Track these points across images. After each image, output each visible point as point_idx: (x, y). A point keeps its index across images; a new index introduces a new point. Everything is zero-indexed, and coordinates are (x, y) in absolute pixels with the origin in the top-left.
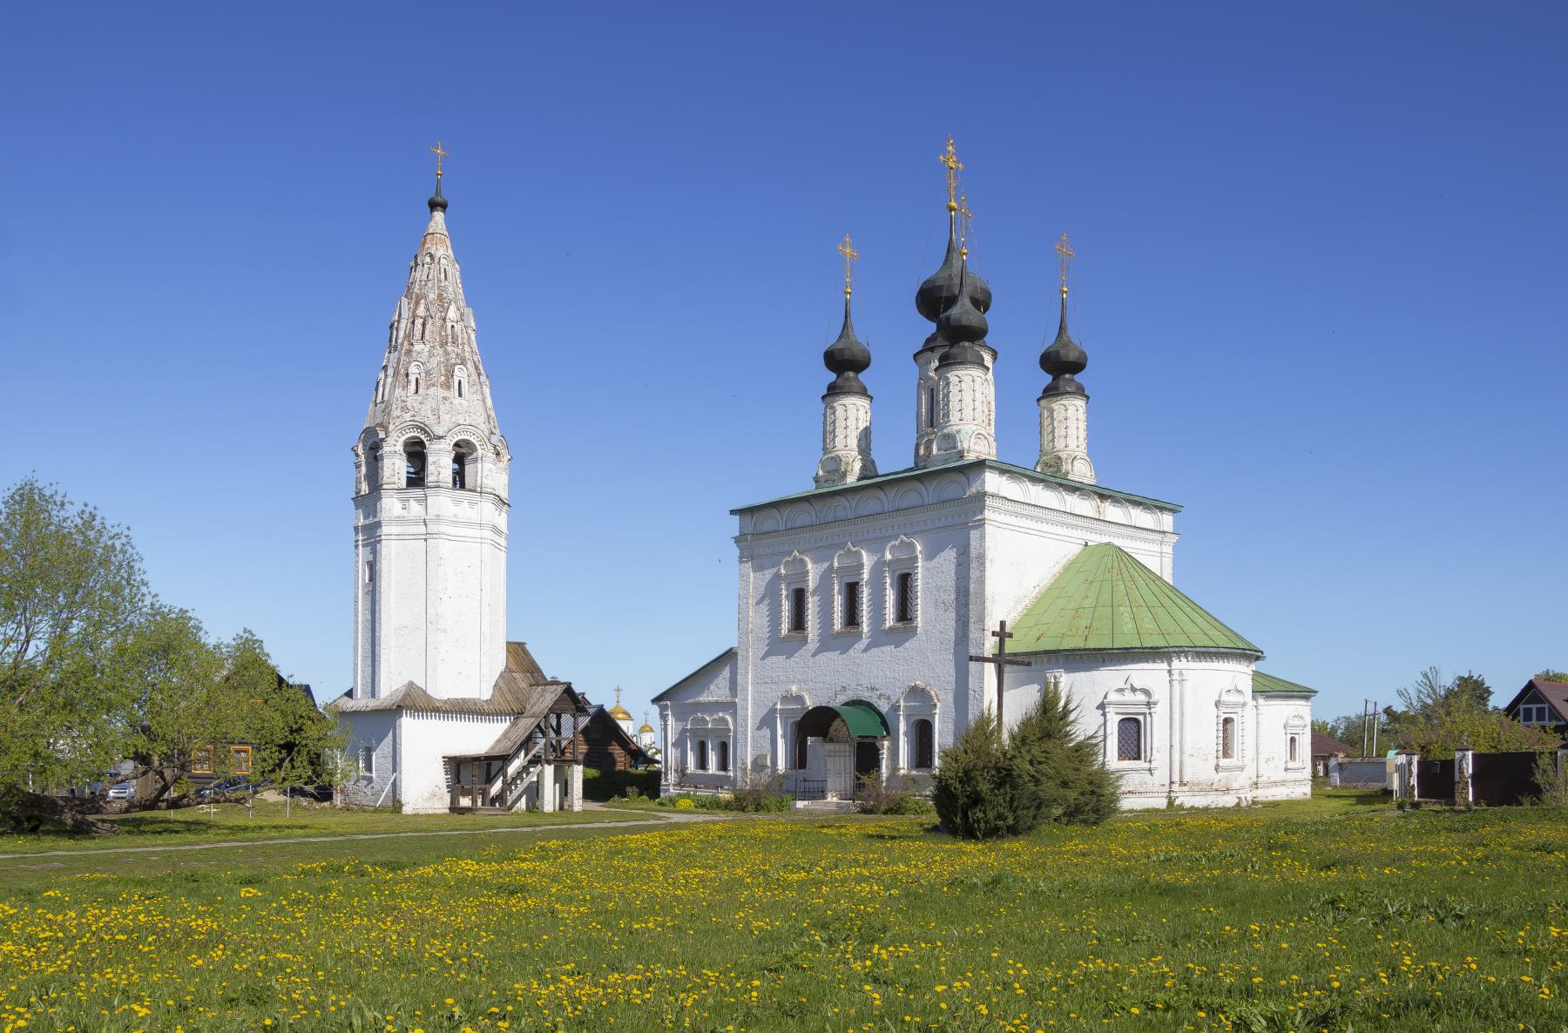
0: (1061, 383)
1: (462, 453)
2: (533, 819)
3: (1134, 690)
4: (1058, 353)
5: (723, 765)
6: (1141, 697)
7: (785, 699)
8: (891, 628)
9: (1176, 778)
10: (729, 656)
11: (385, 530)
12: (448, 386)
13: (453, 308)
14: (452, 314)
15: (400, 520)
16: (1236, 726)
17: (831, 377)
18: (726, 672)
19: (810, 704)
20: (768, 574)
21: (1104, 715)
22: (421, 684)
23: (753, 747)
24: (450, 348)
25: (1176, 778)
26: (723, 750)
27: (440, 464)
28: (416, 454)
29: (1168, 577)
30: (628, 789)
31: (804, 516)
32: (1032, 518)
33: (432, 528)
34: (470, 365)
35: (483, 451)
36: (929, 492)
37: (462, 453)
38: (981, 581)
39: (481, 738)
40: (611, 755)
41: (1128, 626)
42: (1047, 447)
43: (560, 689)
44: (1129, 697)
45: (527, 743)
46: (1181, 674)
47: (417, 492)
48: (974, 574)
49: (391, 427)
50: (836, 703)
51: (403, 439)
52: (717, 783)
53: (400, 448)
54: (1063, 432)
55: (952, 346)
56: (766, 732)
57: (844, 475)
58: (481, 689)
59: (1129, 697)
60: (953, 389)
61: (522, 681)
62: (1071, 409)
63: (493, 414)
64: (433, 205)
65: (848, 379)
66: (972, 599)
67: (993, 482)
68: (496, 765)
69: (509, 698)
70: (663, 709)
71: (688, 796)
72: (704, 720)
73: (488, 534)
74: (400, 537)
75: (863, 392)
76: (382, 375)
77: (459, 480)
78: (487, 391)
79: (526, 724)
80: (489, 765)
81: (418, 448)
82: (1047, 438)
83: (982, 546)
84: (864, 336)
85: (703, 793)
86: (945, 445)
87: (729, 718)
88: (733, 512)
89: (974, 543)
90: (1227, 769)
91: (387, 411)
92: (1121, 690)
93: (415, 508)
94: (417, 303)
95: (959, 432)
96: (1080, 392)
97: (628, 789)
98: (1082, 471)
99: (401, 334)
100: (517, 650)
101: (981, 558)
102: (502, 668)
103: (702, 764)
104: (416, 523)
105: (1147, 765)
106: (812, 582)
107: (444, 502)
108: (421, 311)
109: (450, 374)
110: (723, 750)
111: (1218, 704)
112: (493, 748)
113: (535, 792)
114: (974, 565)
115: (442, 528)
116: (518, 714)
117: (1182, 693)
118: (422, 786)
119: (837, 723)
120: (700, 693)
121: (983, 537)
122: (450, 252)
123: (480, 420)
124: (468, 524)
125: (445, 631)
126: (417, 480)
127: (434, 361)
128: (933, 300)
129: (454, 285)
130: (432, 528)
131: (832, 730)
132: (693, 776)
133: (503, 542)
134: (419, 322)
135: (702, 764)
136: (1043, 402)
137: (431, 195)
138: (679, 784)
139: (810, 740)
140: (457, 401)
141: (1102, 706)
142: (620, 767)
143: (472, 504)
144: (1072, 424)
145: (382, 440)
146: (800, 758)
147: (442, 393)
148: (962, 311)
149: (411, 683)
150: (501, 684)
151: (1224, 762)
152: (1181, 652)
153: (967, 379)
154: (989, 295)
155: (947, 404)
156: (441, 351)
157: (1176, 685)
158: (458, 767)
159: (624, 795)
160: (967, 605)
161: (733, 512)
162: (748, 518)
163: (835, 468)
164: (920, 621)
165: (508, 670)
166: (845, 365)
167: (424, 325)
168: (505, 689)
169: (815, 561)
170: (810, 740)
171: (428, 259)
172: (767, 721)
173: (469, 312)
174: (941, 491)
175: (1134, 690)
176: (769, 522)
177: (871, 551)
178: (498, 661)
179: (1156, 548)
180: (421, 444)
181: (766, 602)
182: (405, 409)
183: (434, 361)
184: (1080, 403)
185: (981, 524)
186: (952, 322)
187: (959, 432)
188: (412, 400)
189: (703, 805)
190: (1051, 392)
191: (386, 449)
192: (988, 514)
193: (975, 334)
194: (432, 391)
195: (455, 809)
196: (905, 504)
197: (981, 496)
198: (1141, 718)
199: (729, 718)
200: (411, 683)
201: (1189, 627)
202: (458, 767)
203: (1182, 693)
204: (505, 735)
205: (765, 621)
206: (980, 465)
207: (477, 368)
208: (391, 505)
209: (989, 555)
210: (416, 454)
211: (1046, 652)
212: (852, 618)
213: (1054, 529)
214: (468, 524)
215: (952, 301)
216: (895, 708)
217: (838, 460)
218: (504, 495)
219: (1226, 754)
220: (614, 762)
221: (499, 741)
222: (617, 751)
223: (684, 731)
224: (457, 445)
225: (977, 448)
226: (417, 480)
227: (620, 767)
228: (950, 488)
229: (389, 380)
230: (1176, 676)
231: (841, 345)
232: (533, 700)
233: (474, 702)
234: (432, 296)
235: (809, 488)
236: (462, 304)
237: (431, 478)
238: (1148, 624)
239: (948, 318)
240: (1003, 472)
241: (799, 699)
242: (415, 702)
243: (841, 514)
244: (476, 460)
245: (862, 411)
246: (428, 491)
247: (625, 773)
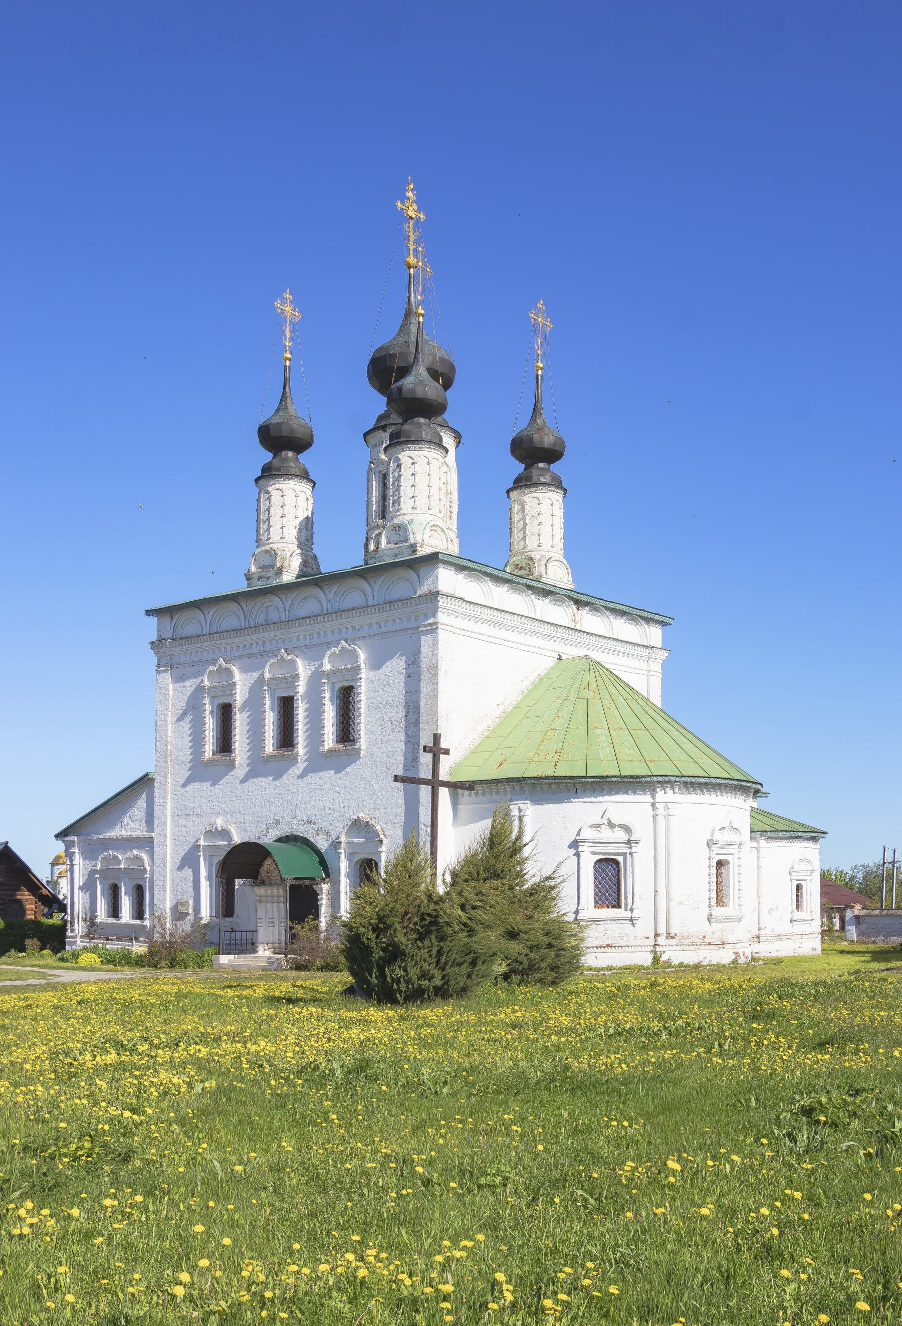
0: (534, 472)
3: (611, 825)
4: (530, 438)
5: (139, 913)
6: (621, 835)
7: (209, 834)
8: (330, 751)
9: (662, 930)
10: (144, 783)
16: (732, 871)
17: (267, 456)
18: (142, 802)
19: (237, 839)
20: (190, 685)
21: (577, 854)
23: (174, 891)
25: (662, 930)
26: (139, 893)
29: (656, 698)
30: (28, 942)
31: (231, 617)
32: (496, 624)
36: (375, 591)
38: (434, 696)
40: (19, 902)
41: (605, 752)
42: (517, 546)
44: (606, 834)
46: (666, 808)
48: (425, 688)
50: (268, 839)
52: (131, 934)
54: (536, 530)
55: (405, 422)
56: (188, 872)
57: (280, 571)
59: (606, 834)
60: (406, 472)
62: (546, 504)
65: (286, 460)
66: (423, 718)
67: (446, 579)
70: (69, 846)
71: (94, 949)
72: (115, 857)
75: (305, 476)
82: (517, 536)
83: (435, 655)
84: (302, 413)
85: (114, 946)
86: (396, 538)
87: (145, 857)
88: (149, 613)
89: (425, 651)
90: (721, 920)
92: (597, 826)
95: (411, 522)
96: (556, 483)
97: (28, 942)
98: (558, 574)
101: (434, 668)
105: (628, 914)
106: (240, 696)
110: (139, 893)
111: (709, 844)
114: (425, 676)
117: (667, 831)
119: (268, 862)
120: (112, 825)
121: (435, 644)
128: (385, 371)
131: (263, 871)
132: (102, 926)
135: (115, 912)
136: (513, 495)
138: (88, 936)
139: (238, 882)
141: (574, 845)
142: (30, 916)
144: (546, 519)
146: (227, 905)
148: (418, 382)
151: (717, 911)
152: (666, 782)
153: (421, 462)
154: (452, 368)
155: (398, 490)
157: (661, 820)
159: (23, 949)
160: (417, 723)
161: (149, 613)
162: (166, 619)
163: (270, 563)
164: (363, 742)
166: (283, 444)
169: (244, 670)
170: (238, 882)
172: (189, 860)
174: (385, 588)
175: (611, 825)
176: (191, 624)
177: (309, 658)
179: (643, 665)
181: (188, 718)
184: (556, 496)
185: (433, 629)
186: (405, 394)
187: (411, 522)
189: (111, 961)
190: (523, 482)
192: (441, 617)
193: (432, 410)
196: (347, 604)
197: (434, 596)
198: (620, 859)
199: (145, 857)
201: (676, 753)
203: (667, 831)
205: (186, 742)
206: (433, 559)
209: (443, 665)
211: (509, 780)
212: (286, 739)
213: (521, 638)
215: (404, 371)
216: (335, 845)
217: (272, 554)
219: (720, 902)
220: (23, 911)
222: (26, 896)
223: (93, 872)
225: (433, 542)
227: (30, 916)
228: (397, 586)
230: (661, 810)
231: (277, 419)
235: (242, 586)
238: (627, 751)
239: (400, 389)
240: (461, 568)
241: (225, 834)
243: (274, 616)
245: (302, 497)
247: (36, 923)
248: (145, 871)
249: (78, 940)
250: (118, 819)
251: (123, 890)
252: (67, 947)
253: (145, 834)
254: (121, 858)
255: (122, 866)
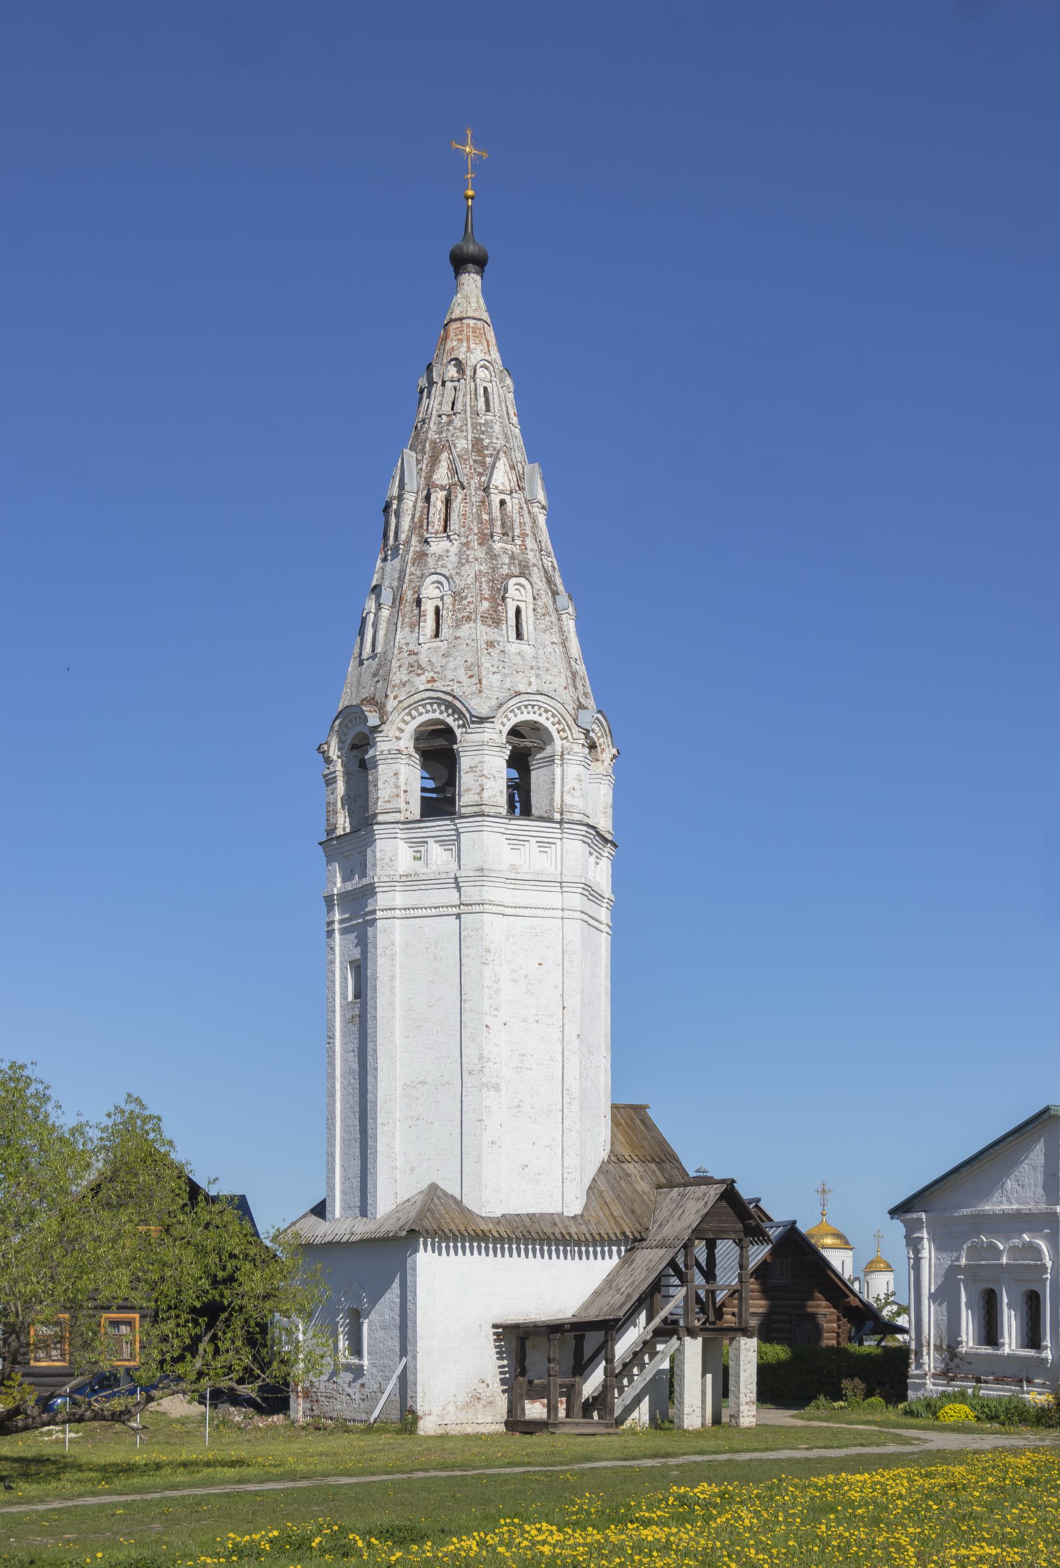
1: (525, 751)
2: (662, 1441)
5: (1032, 1338)
11: (382, 900)
12: (495, 620)
13: (502, 465)
14: (501, 477)
15: (411, 881)
22: (453, 1189)
24: (497, 546)
26: (1032, 1305)
27: (484, 770)
28: (438, 752)
30: (846, 1383)
33: (470, 893)
34: (537, 576)
35: (566, 743)
37: (525, 751)
39: (562, 1288)
40: (813, 1317)
43: (713, 1193)
45: (650, 1297)
47: (441, 826)
49: (391, 704)
51: (414, 724)
52: (1020, 1373)
53: (407, 743)
58: (563, 1195)
61: (641, 1178)
63: (581, 669)
64: (460, 262)
68: (592, 1340)
69: (617, 1210)
70: (912, 1228)
71: (961, 1397)
72: (992, 1247)
73: (575, 900)
74: (410, 913)
76: (371, 605)
77: (520, 800)
78: (570, 625)
79: (651, 1260)
80: (580, 1341)
81: (440, 742)
85: (991, 1392)
91: (382, 674)
93: (439, 856)
94: (434, 460)
97: (846, 1383)
99: (406, 523)
100: (631, 1121)
102: (603, 1154)
103: (990, 1334)
104: (435, 882)
107: (493, 843)
108: (442, 475)
109: (499, 596)
110: (1032, 1305)
112: (586, 1306)
113: (666, 1390)
115: (490, 893)
116: (634, 1242)
118: (456, 1382)
120: (986, 1194)
122: (495, 355)
123: (557, 681)
124: (538, 882)
125: (497, 1088)
126: (440, 802)
127: (469, 572)
129: (504, 422)
130: (470, 893)
132: (970, 1359)
133: (604, 915)
134: (438, 497)
135: (990, 1334)
137: (454, 240)
138: (945, 1374)
140: (514, 647)
142: (829, 1341)
143: (544, 844)
145: (375, 729)
147: (484, 632)
149: (434, 1188)
150: (602, 1185)
156: (480, 553)
158: (519, 1342)
159: (836, 1395)
165: (616, 1158)
167: (448, 502)
168: (609, 1196)
171: (452, 372)
173: (534, 474)
178: (597, 1140)
180: (448, 733)
182: (416, 668)
183: (469, 572)
188: (428, 650)
189: (992, 1415)
191: (383, 745)
194: (466, 629)
195: (516, 1424)
200: (434, 1188)
202: (519, 1342)
204: (610, 1282)
207: (549, 581)
208: (393, 852)
210: (438, 752)
214: (538, 882)
218: (605, 824)
221: (597, 1294)
222: (822, 1309)
223: (953, 1271)
224: (515, 732)
226: (440, 802)
227: (829, 1341)
229: (385, 613)
232: (662, 1214)
233: (552, 1219)
234: (462, 444)
236: (519, 455)
237: (466, 799)
242: (442, 1223)
244: (551, 760)
246: (461, 824)
247: (839, 1352)
248: (1044, 1267)
249: (929, 1381)
250: (997, 1183)
251: (1005, 1300)
252: (911, 1394)
253: (1043, 1207)
254: (1001, 1247)
255: (1004, 1260)
